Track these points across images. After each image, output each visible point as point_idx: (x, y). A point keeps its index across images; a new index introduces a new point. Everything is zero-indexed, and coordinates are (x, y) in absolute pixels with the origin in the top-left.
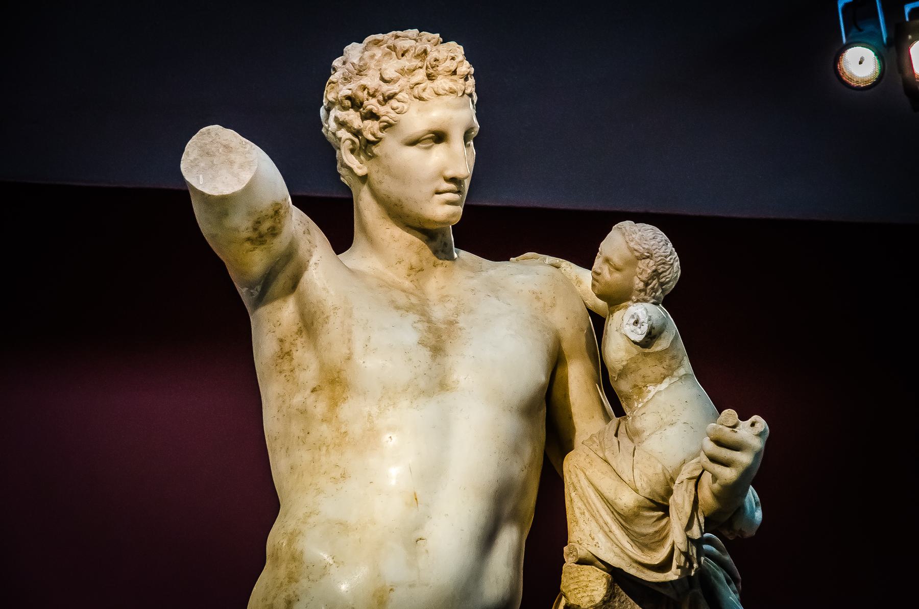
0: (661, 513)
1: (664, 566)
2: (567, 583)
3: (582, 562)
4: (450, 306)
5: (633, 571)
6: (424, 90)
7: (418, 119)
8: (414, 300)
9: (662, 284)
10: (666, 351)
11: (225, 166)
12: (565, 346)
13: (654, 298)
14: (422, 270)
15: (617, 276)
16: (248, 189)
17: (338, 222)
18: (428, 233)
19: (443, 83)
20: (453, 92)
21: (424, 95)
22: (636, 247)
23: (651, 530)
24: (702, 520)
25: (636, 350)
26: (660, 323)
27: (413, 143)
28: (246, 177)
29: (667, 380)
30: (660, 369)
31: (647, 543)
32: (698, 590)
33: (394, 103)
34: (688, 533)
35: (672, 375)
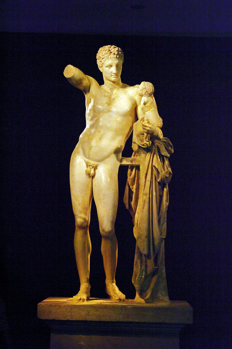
1: (144, 145)
2: (133, 147)
3: (134, 143)
4: (115, 96)
5: (140, 145)
6: (108, 57)
7: (108, 62)
8: (109, 95)
9: (149, 93)
10: (148, 106)
11: (71, 72)
12: (137, 103)
15: (141, 92)
16: (73, 77)
18: (114, 82)
19: (112, 55)
23: (141, 139)
24: (149, 137)
26: (147, 101)
27: (107, 67)
28: (72, 75)
30: (147, 109)
32: (156, 149)
33: (104, 60)
34: (146, 140)
35: (149, 110)
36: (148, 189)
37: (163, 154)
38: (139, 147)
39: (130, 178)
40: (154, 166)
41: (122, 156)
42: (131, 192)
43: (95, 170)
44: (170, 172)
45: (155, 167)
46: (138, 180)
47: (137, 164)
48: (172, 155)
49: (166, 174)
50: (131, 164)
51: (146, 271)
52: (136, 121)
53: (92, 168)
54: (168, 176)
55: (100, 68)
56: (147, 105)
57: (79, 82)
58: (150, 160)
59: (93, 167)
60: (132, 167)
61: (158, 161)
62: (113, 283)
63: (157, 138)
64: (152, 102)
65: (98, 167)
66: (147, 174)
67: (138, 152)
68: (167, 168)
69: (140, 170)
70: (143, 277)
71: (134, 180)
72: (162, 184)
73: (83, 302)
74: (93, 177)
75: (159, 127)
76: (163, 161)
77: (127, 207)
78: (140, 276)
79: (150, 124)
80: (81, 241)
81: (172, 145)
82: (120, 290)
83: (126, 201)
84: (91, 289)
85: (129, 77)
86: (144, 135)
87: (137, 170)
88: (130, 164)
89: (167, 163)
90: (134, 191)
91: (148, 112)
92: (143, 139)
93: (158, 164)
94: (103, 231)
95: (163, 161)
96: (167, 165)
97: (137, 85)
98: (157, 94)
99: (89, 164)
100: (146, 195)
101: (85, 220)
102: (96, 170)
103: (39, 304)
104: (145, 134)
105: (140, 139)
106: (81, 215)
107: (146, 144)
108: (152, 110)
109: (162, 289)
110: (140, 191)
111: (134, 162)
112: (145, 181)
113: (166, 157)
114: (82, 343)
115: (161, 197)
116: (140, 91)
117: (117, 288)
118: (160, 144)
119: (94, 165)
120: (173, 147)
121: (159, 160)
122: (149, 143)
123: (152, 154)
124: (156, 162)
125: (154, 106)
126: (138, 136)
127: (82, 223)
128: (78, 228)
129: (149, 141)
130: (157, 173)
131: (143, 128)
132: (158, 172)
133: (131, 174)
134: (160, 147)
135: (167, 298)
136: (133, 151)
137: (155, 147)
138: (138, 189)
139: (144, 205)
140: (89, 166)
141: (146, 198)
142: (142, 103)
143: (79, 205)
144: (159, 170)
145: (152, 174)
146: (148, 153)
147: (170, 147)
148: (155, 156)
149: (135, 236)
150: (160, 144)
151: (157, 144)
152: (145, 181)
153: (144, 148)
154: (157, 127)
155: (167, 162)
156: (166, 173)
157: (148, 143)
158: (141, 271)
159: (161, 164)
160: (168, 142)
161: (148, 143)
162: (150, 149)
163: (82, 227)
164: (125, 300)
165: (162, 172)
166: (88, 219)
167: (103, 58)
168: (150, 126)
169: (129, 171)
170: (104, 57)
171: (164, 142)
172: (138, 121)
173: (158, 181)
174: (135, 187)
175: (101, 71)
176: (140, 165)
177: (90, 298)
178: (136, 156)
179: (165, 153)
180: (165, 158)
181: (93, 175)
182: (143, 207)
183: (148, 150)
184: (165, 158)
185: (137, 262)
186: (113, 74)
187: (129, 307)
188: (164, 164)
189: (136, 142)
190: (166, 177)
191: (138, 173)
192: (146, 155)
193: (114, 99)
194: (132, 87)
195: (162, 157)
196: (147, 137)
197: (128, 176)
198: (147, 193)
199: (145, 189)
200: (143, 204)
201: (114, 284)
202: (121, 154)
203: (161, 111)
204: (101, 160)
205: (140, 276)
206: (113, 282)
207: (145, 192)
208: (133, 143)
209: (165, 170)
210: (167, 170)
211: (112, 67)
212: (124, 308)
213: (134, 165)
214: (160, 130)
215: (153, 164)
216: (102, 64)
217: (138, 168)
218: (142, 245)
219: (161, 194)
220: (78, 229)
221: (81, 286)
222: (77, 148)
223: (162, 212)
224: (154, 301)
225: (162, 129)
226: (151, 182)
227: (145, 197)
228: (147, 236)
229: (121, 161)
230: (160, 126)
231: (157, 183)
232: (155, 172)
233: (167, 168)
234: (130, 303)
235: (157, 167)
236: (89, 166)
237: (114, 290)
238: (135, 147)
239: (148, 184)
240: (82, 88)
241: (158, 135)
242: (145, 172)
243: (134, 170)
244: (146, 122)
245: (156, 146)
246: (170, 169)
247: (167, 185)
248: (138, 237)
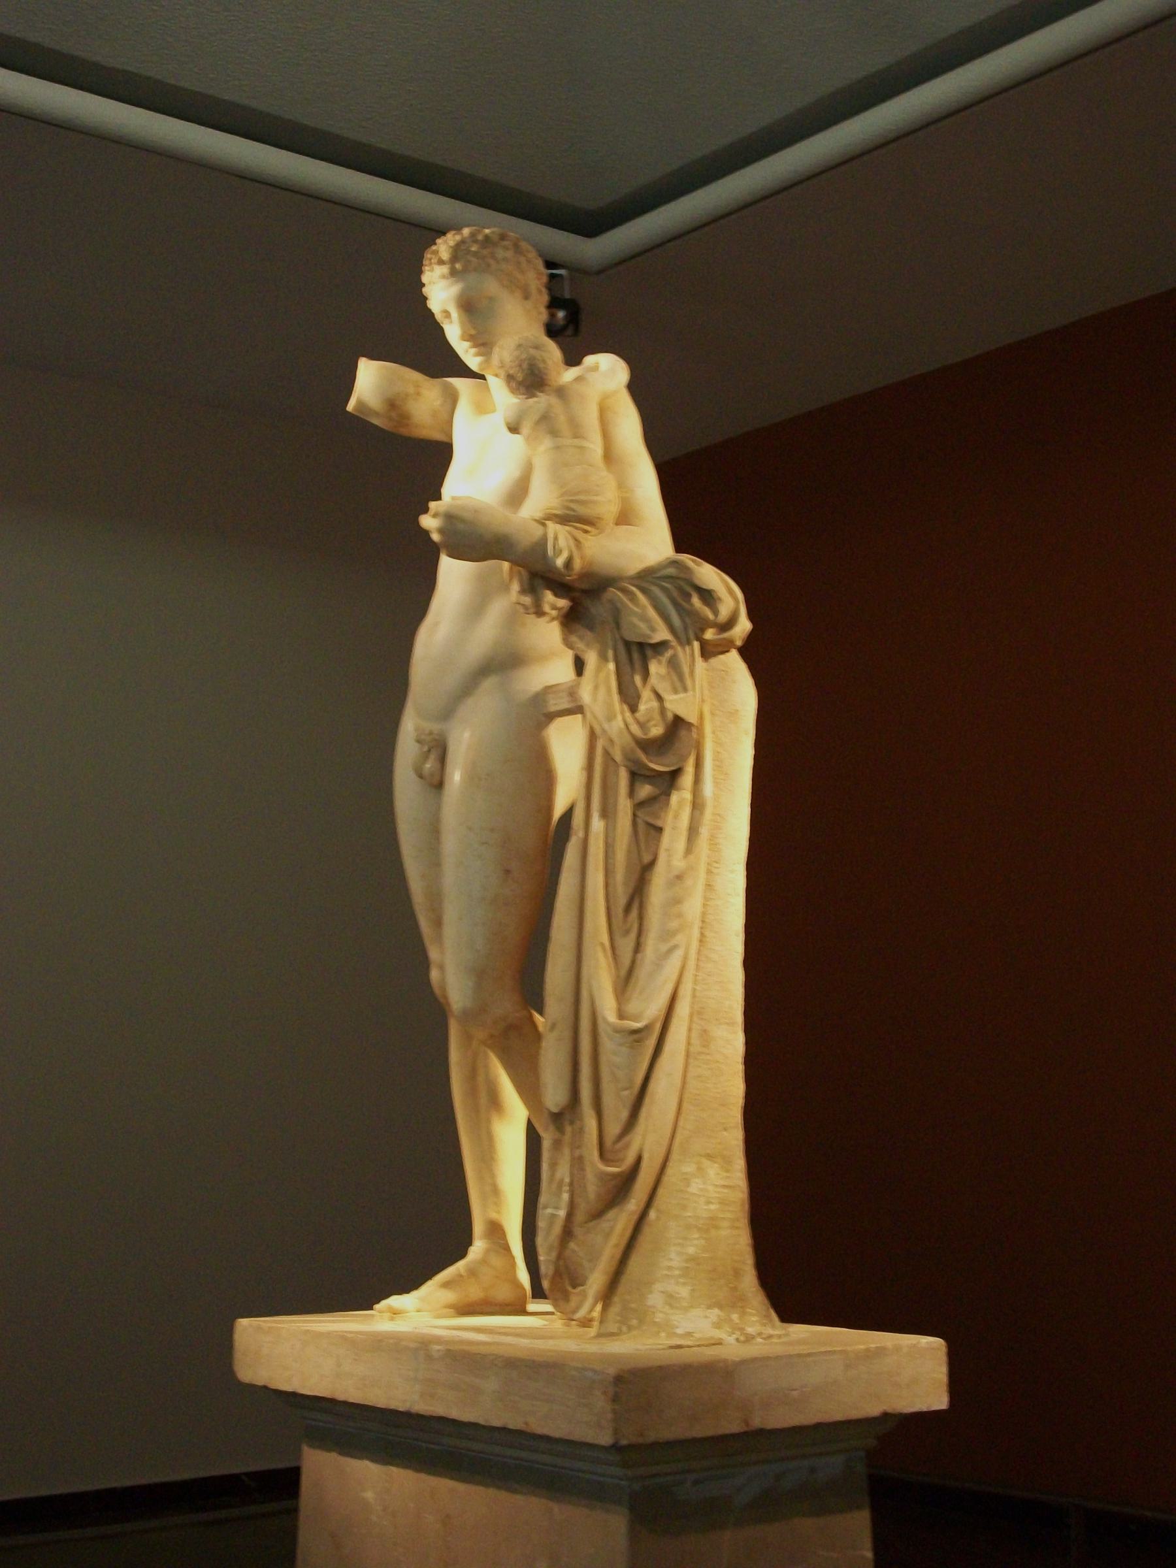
49: (635, 729)
56: (526, 428)
57: (393, 414)
61: (602, 675)
73: (392, 1319)
75: (556, 516)
114: (369, 1495)
121: (611, 666)
165: (611, 718)
177: (532, 1307)
187: (437, 1347)
210: (655, 704)
219: (659, 823)
231: (623, 777)
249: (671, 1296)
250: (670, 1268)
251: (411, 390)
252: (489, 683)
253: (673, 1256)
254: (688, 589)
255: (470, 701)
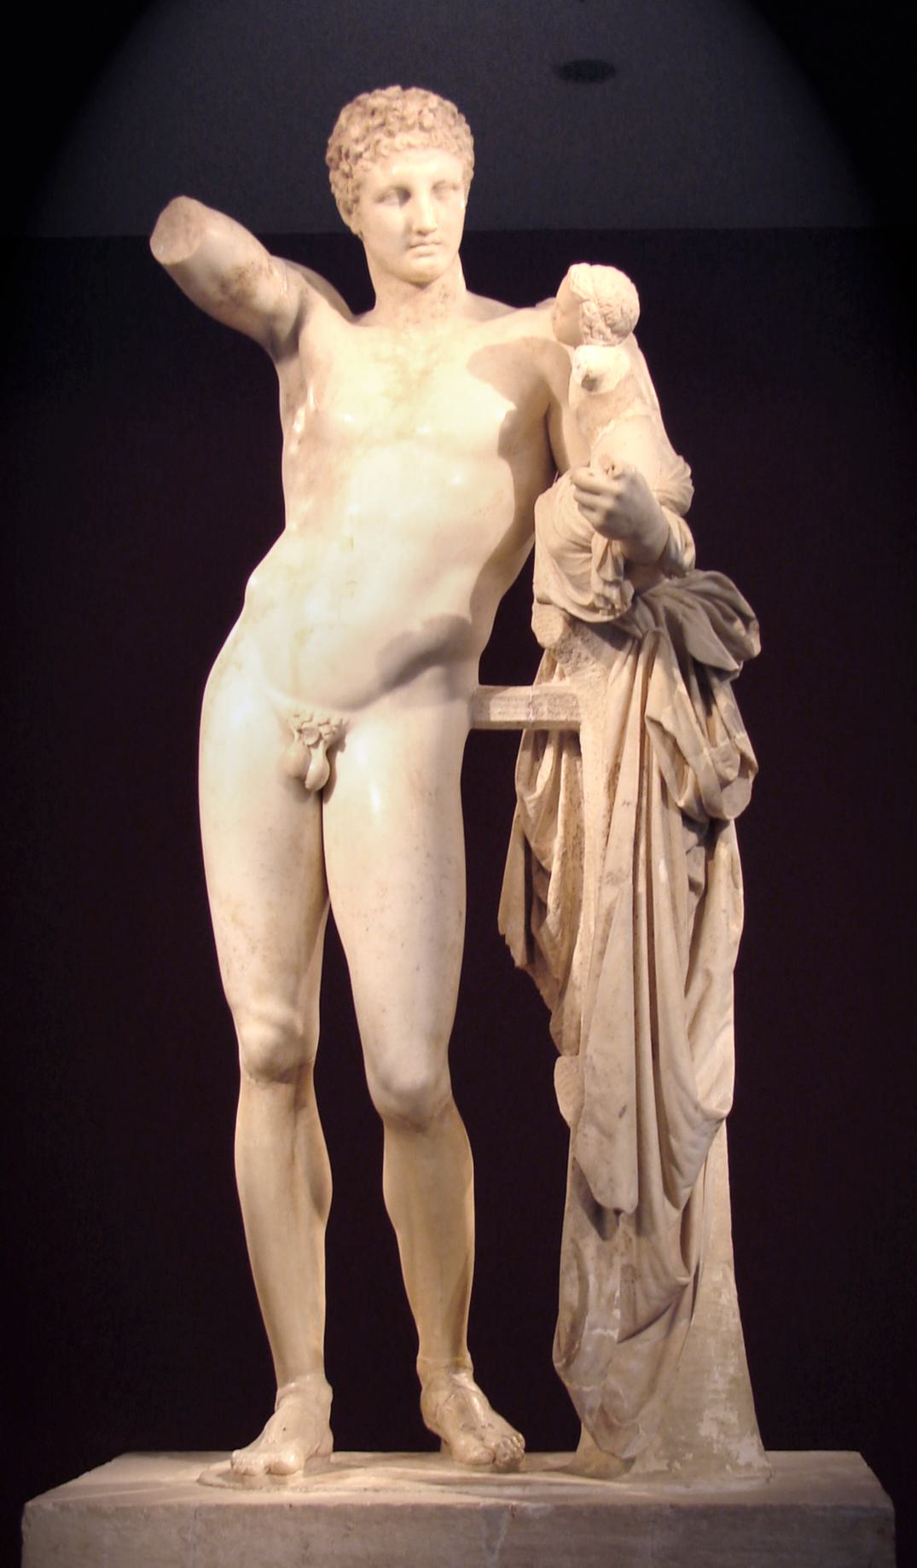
0: (585, 555)
1: (593, 608)
2: (536, 625)
3: (541, 602)
12: (556, 389)
13: (605, 339)
14: (418, 322)
17: (350, 278)
20: (410, 146)
21: (385, 152)
22: (575, 289)
23: (578, 572)
25: (583, 393)
27: (382, 199)
29: (612, 424)
31: (580, 584)
32: (664, 630)
33: (361, 162)
34: (603, 575)
36: (628, 848)
37: (702, 657)
38: (573, 622)
39: (530, 796)
40: (652, 721)
41: (482, 682)
42: (535, 871)
43: (330, 754)
44: (743, 757)
45: (659, 724)
46: (575, 804)
47: (563, 718)
48: (751, 665)
49: (720, 766)
50: (532, 718)
51: (630, 1303)
52: (549, 485)
53: (316, 745)
54: (732, 773)
55: (349, 212)
56: (606, 387)
57: (235, 288)
58: (631, 690)
59: (320, 737)
60: (541, 737)
61: (675, 696)
62: (456, 1372)
63: (666, 564)
64: (630, 377)
65: (348, 740)
66: (616, 769)
67: (563, 650)
68: (728, 733)
69: (579, 754)
70: (615, 1334)
71: (552, 809)
72: (704, 824)
74: (323, 793)
75: (672, 502)
76: (708, 699)
77: (518, 954)
78: (599, 1331)
79: (617, 478)
80: (271, 1151)
81: (750, 611)
82: (499, 1403)
83: (511, 924)
84: (335, 1406)
85: (509, 260)
86: (589, 550)
87: (564, 756)
88: (522, 718)
89: (728, 706)
90: (555, 868)
91: (607, 429)
92: (588, 573)
93: (675, 711)
94: (386, 1086)
95: (708, 699)
96: (725, 716)
97: (549, 300)
98: (655, 335)
99: (296, 724)
100: (613, 879)
101: (287, 1030)
102: (340, 757)
103: (29, 1504)
104: (599, 542)
105: (571, 578)
106: (262, 1007)
107: (607, 600)
108: (630, 413)
109: (724, 1396)
110: (585, 867)
111: (545, 708)
112: (611, 810)
113: (721, 673)
115: (702, 892)
116: (564, 314)
117: (478, 1401)
118: (682, 602)
119: (324, 730)
120: (755, 624)
121: (682, 688)
122: (622, 595)
123: (642, 658)
124: (667, 694)
125: (640, 395)
126: (559, 558)
127: (276, 1050)
128: (251, 1075)
129: (616, 583)
130: (673, 760)
131: (585, 507)
132: (676, 751)
133: (536, 778)
134: (680, 617)
135: (748, 1448)
136: (539, 650)
137: (657, 624)
138: (574, 849)
139: (605, 939)
140: (297, 735)
141: (618, 896)
142: (576, 378)
143: (254, 949)
144: (683, 743)
145: (644, 768)
146: (622, 654)
147: (738, 624)
148: (658, 668)
149: (566, 1110)
150: (682, 602)
151: (664, 602)
152: (611, 810)
153: (599, 629)
154: (662, 504)
155: (725, 700)
156: (724, 761)
157: (613, 593)
158: (603, 1301)
159: (692, 710)
160: (728, 594)
161: (613, 593)
162: (627, 628)
163: (272, 1073)
164: (523, 1465)
165: (698, 751)
166: (307, 1024)
167: (359, 156)
168: (617, 487)
169: (523, 758)
170: (360, 148)
171: (707, 595)
172: (563, 485)
173: (681, 804)
174: (557, 845)
175: (355, 230)
176: (578, 724)
178: (556, 677)
179: (707, 647)
180: (715, 681)
181: (323, 783)
182: (598, 945)
183: (617, 633)
184: (715, 681)
185: (578, 1255)
186: (416, 239)
188: (709, 713)
189: (555, 596)
190: (725, 783)
191: (573, 772)
192: (610, 667)
193: (425, 373)
194: (525, 313)
195: (700, 676)
196: (609, 561)
197: (519, 787)
198: (620, 870)
199: (611, 853)
200: (600, 932)
201: (466, 1379)
202: (472, 670)
203: (683, 426)
204: (361, 702)
205: (599, 1331)
206: (457, 1367)
207: (609, 866)
208: (535, 606)
209: (720, 747)
211: (411, 201)
212: (507, 1515)
213: (548, 722)
214: (682, 521)
215: (647, 712)
216: (358, 186)
217: (570, 740)
218: (603, 1156)
219: (701, 879)
220: (253, 1081)
221: (279, 1392)
222: (236, 642)
223: (708, 975)
224: (677, 1465)
225: (691, 517)
226: (642, 814)
227: (610, 894)
228: (624, 1109)
229: (477, 705)
230: (677, 498)
231: (677, 819)
232: (659, 757)
233: (728, 733)
234: (552, 1481)
235: (669, 725)
236: (300, 731)
237: (464, 1409)
238: (546, 627)
239: (625, 819)
240: (255, 329)
241: (666, 549)
242: (608, 761)
243: (549, 753)
244: (596, 468)
245: (663, 617)
246: (743, 740)
247: (731, 832)
248: (578, 1114)
249: (723, 1423)
250: (716, 1391)
251: (265, 264)
252: (431, 674)
253: (717, 1376)
254: (733, 614)
255: (402, 693)
